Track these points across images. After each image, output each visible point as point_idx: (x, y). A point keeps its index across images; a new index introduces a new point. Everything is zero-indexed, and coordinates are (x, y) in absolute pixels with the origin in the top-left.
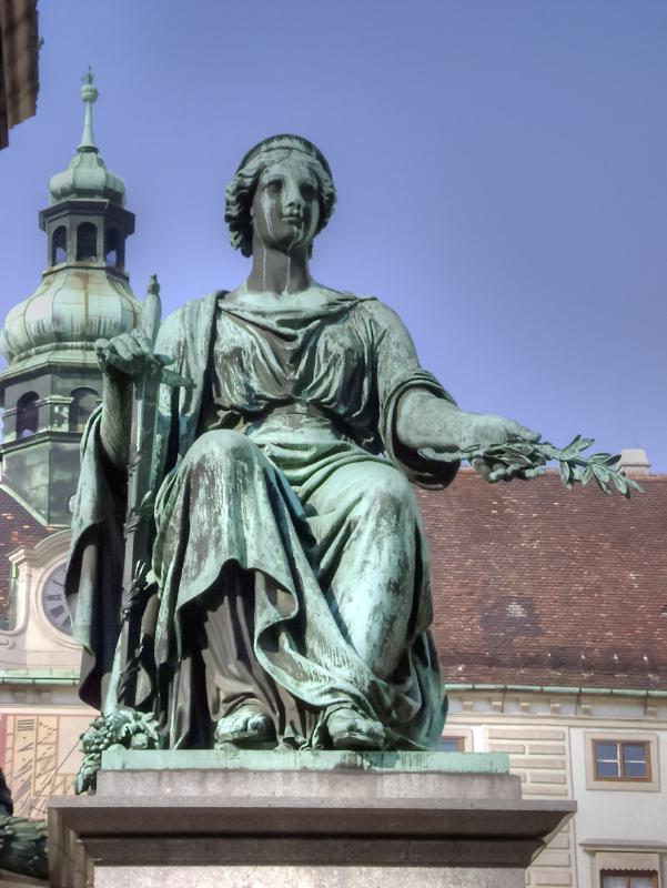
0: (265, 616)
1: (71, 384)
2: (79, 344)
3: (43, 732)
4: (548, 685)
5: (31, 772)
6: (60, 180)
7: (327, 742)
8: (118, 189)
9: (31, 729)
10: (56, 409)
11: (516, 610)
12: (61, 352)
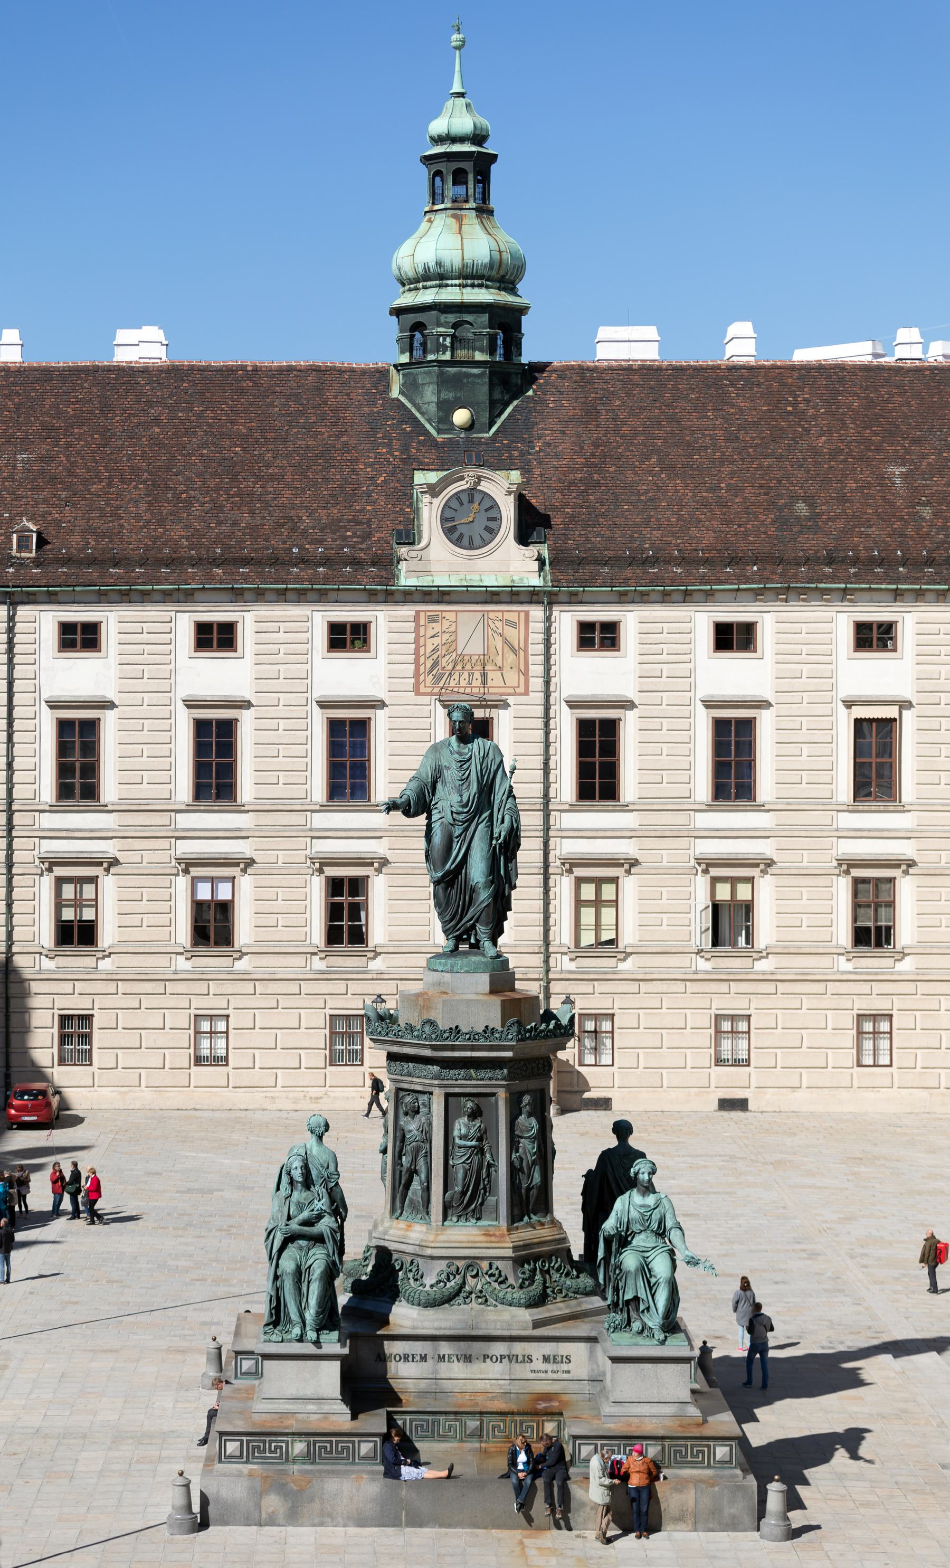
1: (452, 318)
2: (457, 282)
3: (446, 624)
4: (820, 583)
5: (439, 653)
6: (438, 126)
8: (484, 133)
9: (436, 621)
10: (441, 339)
12: (443, 290)
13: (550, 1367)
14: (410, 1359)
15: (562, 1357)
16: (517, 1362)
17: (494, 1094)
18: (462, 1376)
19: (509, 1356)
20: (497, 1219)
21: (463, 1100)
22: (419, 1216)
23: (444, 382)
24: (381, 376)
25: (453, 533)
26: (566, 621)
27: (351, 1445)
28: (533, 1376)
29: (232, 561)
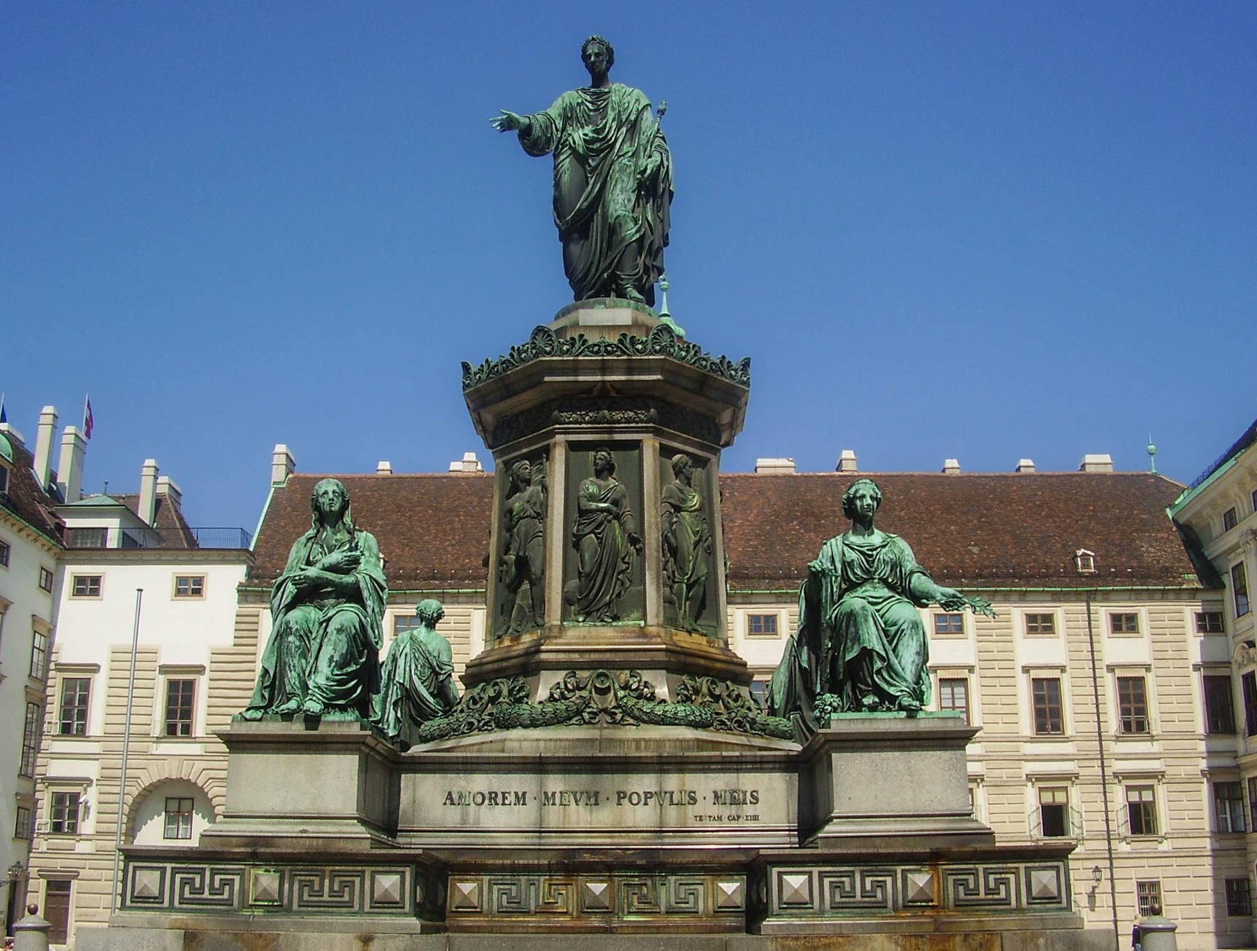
0: (878, 664)
7: (901, 708)
14: (500, 800)
15: (745, 793)
16: (672, 803)
17: (637, 445)
18: (583, 825)
19: (659, 794)
20: (644, 617)
21: (593, 453)
22: (530, 625)
27: (357, 880)
28: (697, 825)
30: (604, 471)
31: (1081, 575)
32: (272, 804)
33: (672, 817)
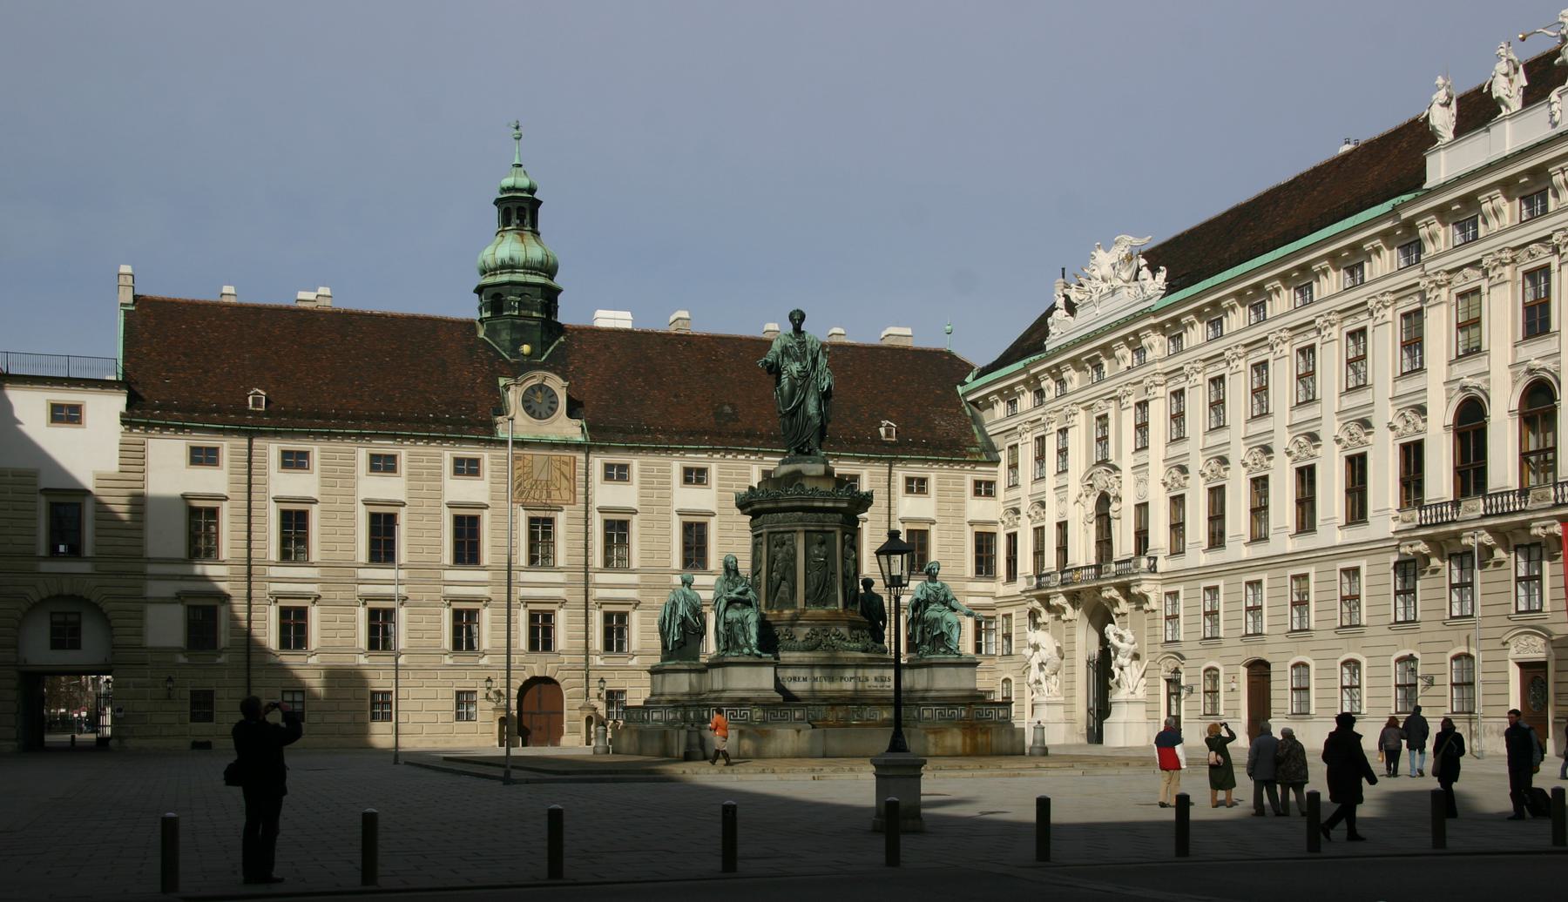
6: (508, 182)
11: (727, 409)
13: (879, 684)
23: (514, 328)
24: (470, 325)
25: (529, 407)
26: (598, 462)
29: (392, 419)
30: (822, 543)
31: (885, 443)
32: (744, 685)
33: (860, 686)
